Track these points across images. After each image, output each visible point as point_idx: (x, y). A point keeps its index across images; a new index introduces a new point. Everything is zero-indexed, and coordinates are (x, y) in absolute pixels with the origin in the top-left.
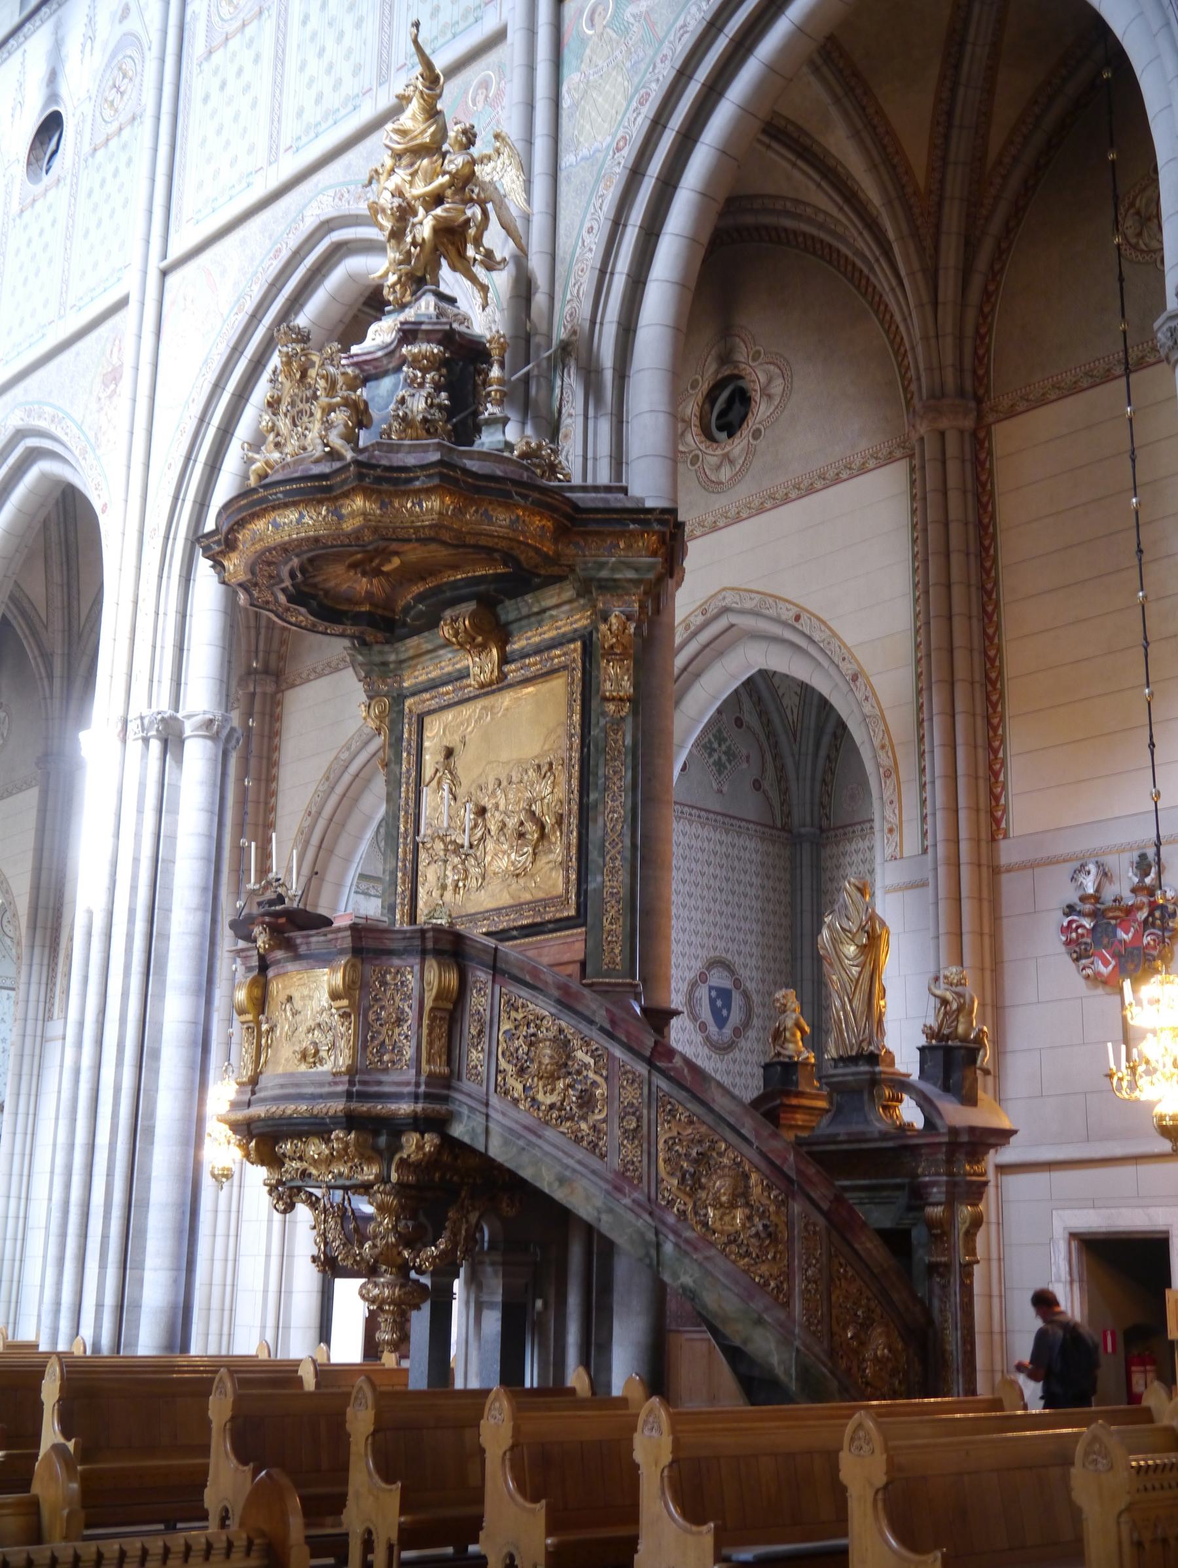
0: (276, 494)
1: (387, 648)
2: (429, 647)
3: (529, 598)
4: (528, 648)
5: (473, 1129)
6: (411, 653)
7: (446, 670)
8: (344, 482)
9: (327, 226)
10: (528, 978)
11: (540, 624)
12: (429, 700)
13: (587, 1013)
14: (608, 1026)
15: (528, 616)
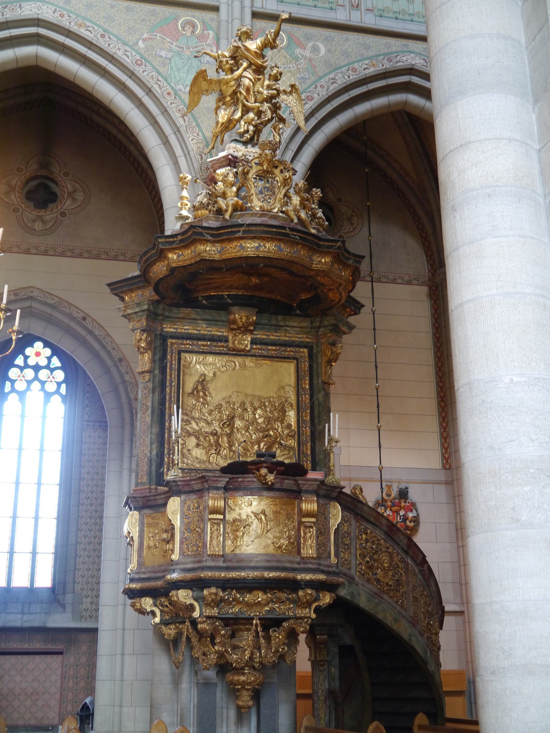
0: (295, 235)
1: (167, 308)
3: (280, 318)
4: (267, 340)
6: (181, 315)
7: (202, 332)
8: (332, 247)
9: (38, 22)
12: (188, 344)
13: (398, 540)
14: (405, 549)
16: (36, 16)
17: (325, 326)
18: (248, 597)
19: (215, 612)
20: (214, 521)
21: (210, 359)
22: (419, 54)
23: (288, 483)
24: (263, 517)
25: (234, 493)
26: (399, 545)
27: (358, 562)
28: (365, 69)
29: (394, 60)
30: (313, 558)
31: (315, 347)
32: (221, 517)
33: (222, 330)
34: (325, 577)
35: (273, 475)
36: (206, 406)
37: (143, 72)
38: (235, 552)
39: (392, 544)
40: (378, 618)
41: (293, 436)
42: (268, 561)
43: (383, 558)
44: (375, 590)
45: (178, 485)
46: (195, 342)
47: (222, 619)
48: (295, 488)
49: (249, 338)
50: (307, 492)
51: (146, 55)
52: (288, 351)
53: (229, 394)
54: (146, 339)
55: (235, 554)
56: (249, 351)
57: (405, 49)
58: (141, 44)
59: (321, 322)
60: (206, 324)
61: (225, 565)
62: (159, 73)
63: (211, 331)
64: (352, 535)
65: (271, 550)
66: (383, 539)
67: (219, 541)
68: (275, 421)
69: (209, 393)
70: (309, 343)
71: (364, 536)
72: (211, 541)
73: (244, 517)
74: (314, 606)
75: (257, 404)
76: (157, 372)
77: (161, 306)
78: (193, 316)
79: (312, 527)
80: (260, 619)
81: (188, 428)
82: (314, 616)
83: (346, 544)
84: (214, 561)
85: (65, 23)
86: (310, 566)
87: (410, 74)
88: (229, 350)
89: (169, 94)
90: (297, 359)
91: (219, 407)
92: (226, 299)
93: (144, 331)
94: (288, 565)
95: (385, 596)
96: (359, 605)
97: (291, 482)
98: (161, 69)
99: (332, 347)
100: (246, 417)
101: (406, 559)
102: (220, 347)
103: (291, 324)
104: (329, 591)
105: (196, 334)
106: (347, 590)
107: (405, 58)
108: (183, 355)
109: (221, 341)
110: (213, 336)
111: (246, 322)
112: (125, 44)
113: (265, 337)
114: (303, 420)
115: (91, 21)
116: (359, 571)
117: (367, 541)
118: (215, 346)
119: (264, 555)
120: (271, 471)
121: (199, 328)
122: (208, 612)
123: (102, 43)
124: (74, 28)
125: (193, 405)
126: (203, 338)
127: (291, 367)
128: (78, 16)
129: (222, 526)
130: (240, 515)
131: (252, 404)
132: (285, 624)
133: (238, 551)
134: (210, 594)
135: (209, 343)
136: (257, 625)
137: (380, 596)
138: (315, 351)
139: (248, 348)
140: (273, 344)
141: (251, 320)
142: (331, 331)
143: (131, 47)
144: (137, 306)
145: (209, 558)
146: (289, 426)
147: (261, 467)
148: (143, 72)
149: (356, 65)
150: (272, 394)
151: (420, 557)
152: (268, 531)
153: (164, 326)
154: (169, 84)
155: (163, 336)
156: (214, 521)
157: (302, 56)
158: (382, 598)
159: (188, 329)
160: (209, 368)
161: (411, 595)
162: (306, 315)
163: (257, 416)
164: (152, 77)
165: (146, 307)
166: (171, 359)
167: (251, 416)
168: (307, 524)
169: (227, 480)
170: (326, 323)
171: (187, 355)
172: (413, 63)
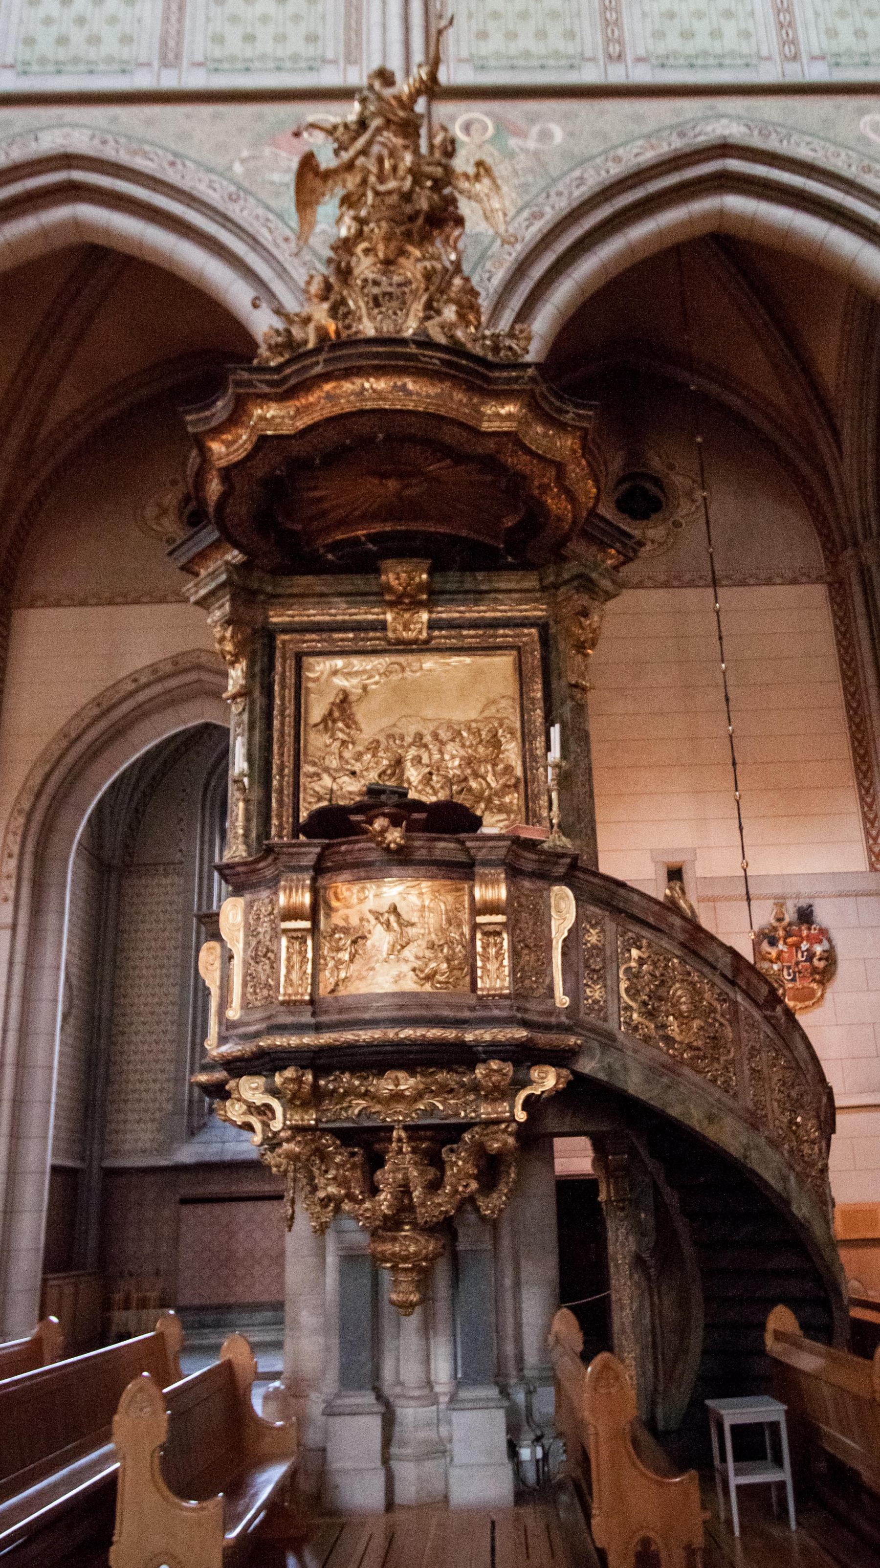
1: (268, 577)
2: (325, 590)
3: (480, 576)
5: (610, 1066)
6: (296, 590)
7: (339, 618)
10: (651, 920)
11: (476, 602)
12: (312, 641)
15: (467, 592)
16: (61, 150)
17: (566, 582)
18: (385, 1085)
19: (310, 1118)
20: (295, 934)
21: (358, 663)
22: (739, 118)
23: (445, 847)
24: (392, 919)
25: (334, 878)
26: (714, 968)
27: (623, 1005)
28: (637, 155)
29: (691, 134)
30: (501, 996)
31: (552, 623)
32: (307, 924)
33: (376, 610)
34: (525, 1034)
35: (399, 829)
36: (350, 746)
37: (242, 210)
38: (336, 994)
39: (698, 966)
40: (670, 1116)
41: (516, 786)
42: (401, 1007)
43: (679, 993)
44: (664, 1059)
45: (238, 874)
46: (325, 636)
47: (337, 1133)
48: (462, 858)
49: (425, 616)
50: (486, 863)
51: (246, 184)
52: (502, 636)
53: (392, 722)
54: (232, 637)
55: (336, 999)
56: (427, 642)
57: (710, 113)
58: (238, 168)
59: (558, 575)
60: (347, 602)
61: (312, 1021)
62: (268, 208)
63: (355, 614)
64: (608, 953)
65: (410, 984)
66: (677, 957)
67: (305, 973)
68: (480, 762)
69: (355, 723)
70: (540, 618)
71: (635, 953)
72: (289, 972)
73: (354, 921)
74: (522, 1095)
75: (444, 735)
76: (257, 693)
77: (256, 574)
78: (319, 589)
79: (499, 934)
80: (406, 1128)
81: (318, 789)
82: (521, 1116)
83: (594, 971)
84: (292, 1013)
85: (109, 153)
86: (497, 1013)
87: (724, 156)
88: (389, 643)
89: (287, 240)
90: (519, 649)
91: (374, 747)
92: (364, 544)
93: (229, 622)
94: (447, 1013)
95: (686, 1071)
96: (626, 1091)
97: (452, 845)
98: (272, 203)
99: (582, 619)
100: (425, 759)
101: (732, 995)
102: (373, 639)
103: (503, 586)
104: (553, 1065)
105: (328, 623)
106: (599, 1062)
107: (709, 128)
108: (304, 659)
109: (374, 629)
110: (358, 622)
111: (409, 584)
112: (210, 170)
113: (457, 615)
114: (532, 755)
115: (152, 144)
116: (625, 1022)
117: (641, 961)
118: (362, 640)
119: (394, 995)
120: (395, 822)
121: (333, 611)
122: (297, 1119)
123: (172, 176)
124: (124, 158)
125: (327, 746)
126: (343, 627)
127: (504, 663)
128: (129, 137)
129: (309, 942)
130: (346, 919)
131: (435, 736)
132: (467, 1137)
133: (342, 992)
134: (287, 1080)
135: (351, 635)
136: (400, 1140)
137: (673, 1072)
138: (553, 630)
139: (424, 635)
140: (474, 625)
141: (417, 580)
142: (577, 590)
143: (221, 175)
144: (213, 580)
145: (282, 1009)
146: (508, 769)
147: (376, 816)
148: (242, 210)
149: (620, 152)
150: (473, 715)
151: (764, 990)
152: (403, 947)
153: (271, 613)
154: (286, 224)
155: (268, 630)
156: (295, 934)
157: (522, 149)
158: (679, 1075)
159: (314, 615)
160: (355, 681)
161: (746, 1068)
162: (524, 566)
163: (447, 757)
164: (257, 217)
165: (224, 577)
166: (283, 668)
167: (437, 756)
168: (491, 928)
169: (318, 850)
170: (566, 576)
171: (312, 660)
172: (726, 132)
